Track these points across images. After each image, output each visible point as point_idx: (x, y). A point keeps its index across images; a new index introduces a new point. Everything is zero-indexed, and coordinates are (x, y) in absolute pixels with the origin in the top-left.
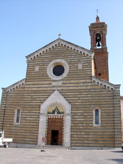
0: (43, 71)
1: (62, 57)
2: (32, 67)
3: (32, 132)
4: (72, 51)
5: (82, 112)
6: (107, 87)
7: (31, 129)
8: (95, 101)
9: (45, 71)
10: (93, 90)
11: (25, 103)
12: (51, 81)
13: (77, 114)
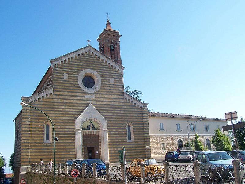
0: (74, 80)
1: (93, 68)
2: (60, 74)
3: (68, 150)
4: (103, 63)
5: (117, 128)
6: (137, 105)
7: (66, 147)
8: (128, 117)
9: (76, 81)
10: (125, 107)
11: (55, 117)
12: (84, 94)
13: (112, 130)
